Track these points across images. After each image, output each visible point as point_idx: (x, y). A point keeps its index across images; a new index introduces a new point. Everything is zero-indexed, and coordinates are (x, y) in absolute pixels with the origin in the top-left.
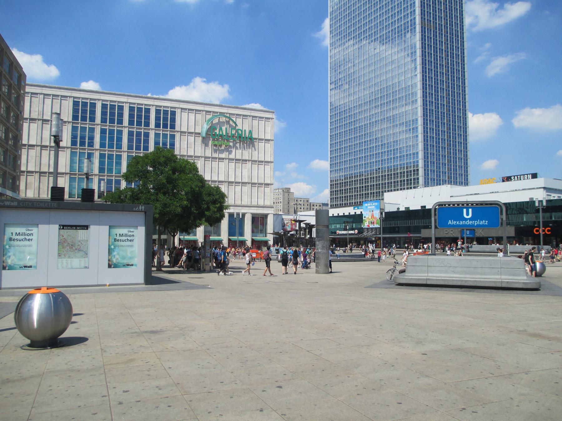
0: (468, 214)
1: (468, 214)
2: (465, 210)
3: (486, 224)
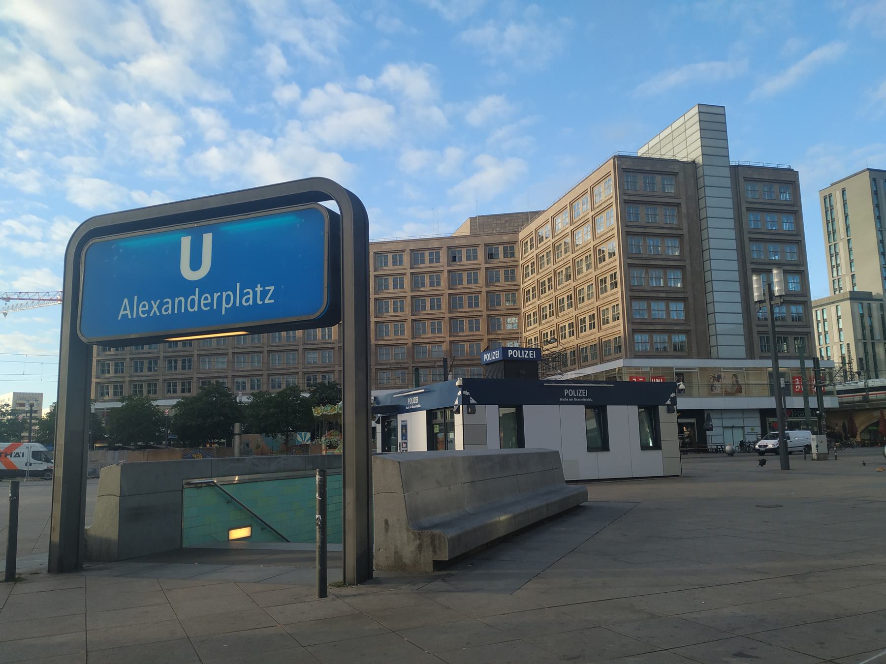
0: (196, 264)
1: (196, 264)
2: (186, 242)
3: (267, 301)
